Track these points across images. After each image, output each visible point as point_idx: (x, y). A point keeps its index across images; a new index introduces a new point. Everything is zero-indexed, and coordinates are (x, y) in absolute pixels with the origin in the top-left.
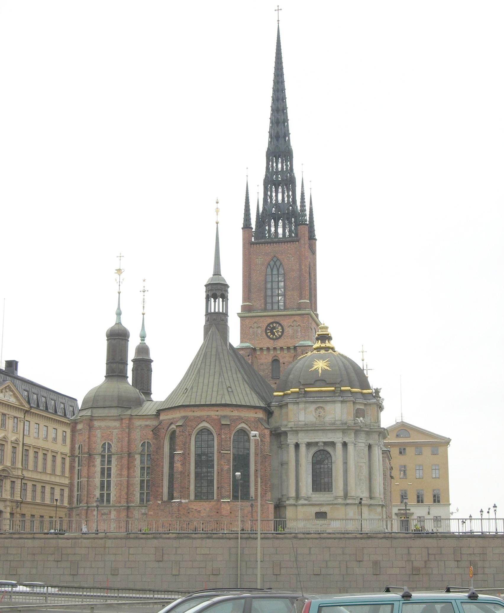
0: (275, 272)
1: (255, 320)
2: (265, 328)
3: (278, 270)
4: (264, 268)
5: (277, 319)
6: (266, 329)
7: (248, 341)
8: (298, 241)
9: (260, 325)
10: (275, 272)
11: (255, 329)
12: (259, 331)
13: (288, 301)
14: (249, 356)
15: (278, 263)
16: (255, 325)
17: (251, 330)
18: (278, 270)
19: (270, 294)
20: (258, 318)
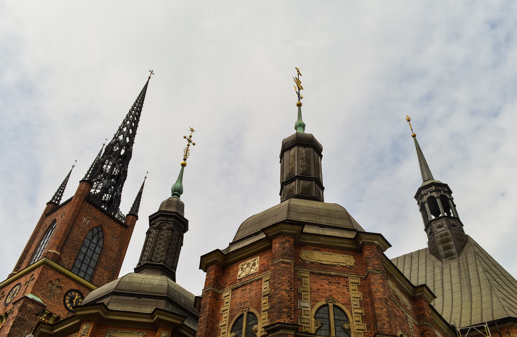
0: (95, 241)
1: (60, 277)
2: (65, 292)
3: (98, 241)
4: (87, 229)
5: (82, 289)
6: (66, 294)
7: (40, 296)
8: (126, 228)
9: (62, 285)
10: (95, 241)
11: (54, 287)
12: (59, 291)
13: (96, 277)
14: (37, 315)
15: (101, 235)
16: (57, 283)
17: (50, 285)
18: (98, 241)
19: (82, 259)
20: (63, 276)
